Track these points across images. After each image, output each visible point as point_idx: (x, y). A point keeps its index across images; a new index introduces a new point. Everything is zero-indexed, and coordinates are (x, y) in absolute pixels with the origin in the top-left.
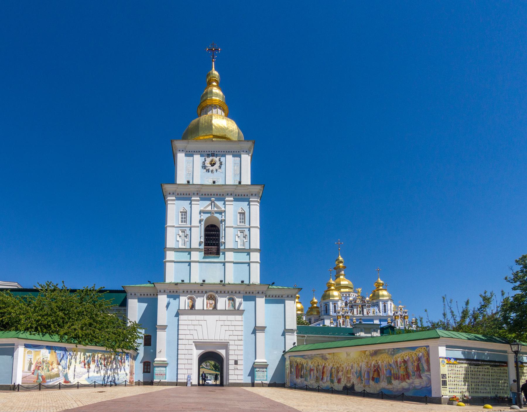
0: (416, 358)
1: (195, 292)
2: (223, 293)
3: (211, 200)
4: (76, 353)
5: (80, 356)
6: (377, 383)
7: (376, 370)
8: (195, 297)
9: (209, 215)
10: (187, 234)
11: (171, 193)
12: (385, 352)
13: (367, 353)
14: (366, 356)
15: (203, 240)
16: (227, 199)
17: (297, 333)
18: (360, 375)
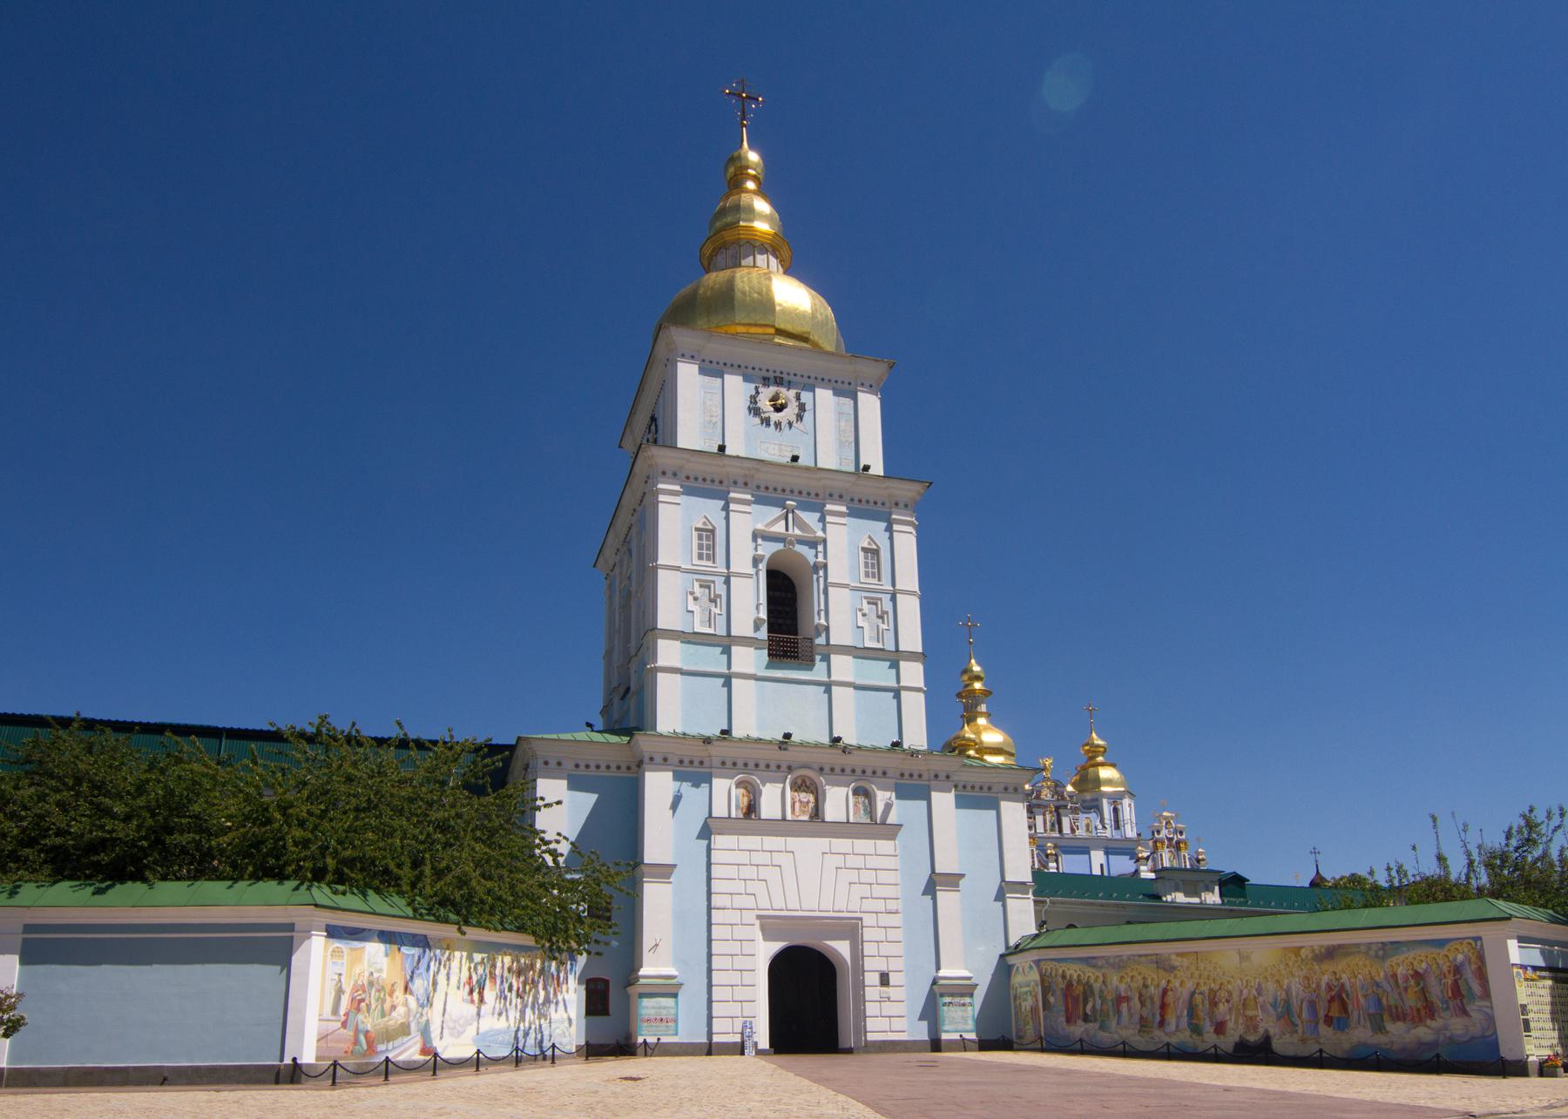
0: (1450, 967)
1: (757, 765)
2: (838, 774)
3: (784, 507)
4: (450, 955)
5: (461, 962)
6: (1343, 1030)
7: (1336, 999)
8: (758, 781)
9: (780, 546)
11: (669, 473)
12: (1359, 952)
13: (1303, 951)
14: (1302, 960)
15: (763, 615)
16: (829, 507)
17: (1034, 894)
18: (1286, 1011)
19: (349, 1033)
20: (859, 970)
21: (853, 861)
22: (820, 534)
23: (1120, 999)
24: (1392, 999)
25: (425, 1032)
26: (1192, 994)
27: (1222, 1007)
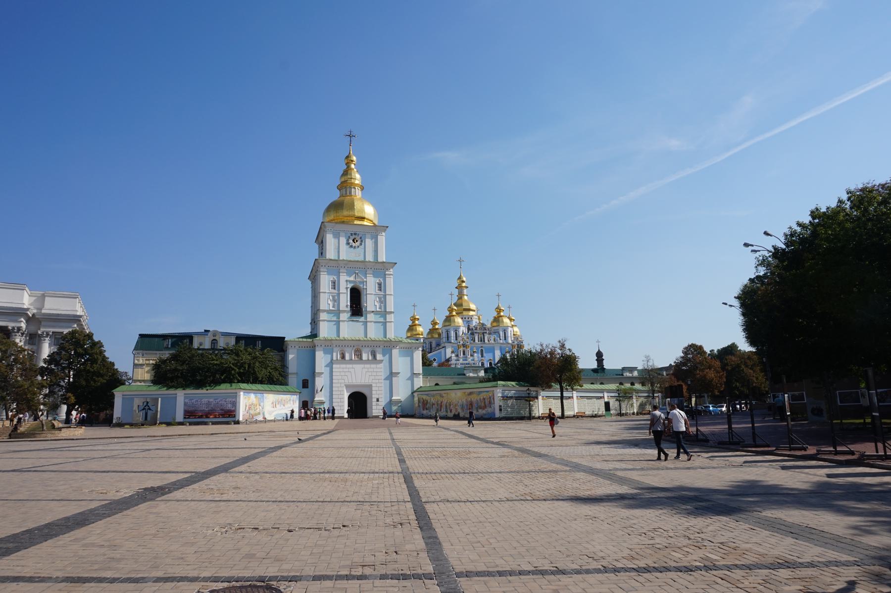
10: (336, 300)
19: (248, 414)
20: (372, 398)
21: (370, 370)
22: (365, 280)
23: (433, 404)
24: (480, 404)
25: (264, 414)
26: (446, 403)
27: (452, 406)
